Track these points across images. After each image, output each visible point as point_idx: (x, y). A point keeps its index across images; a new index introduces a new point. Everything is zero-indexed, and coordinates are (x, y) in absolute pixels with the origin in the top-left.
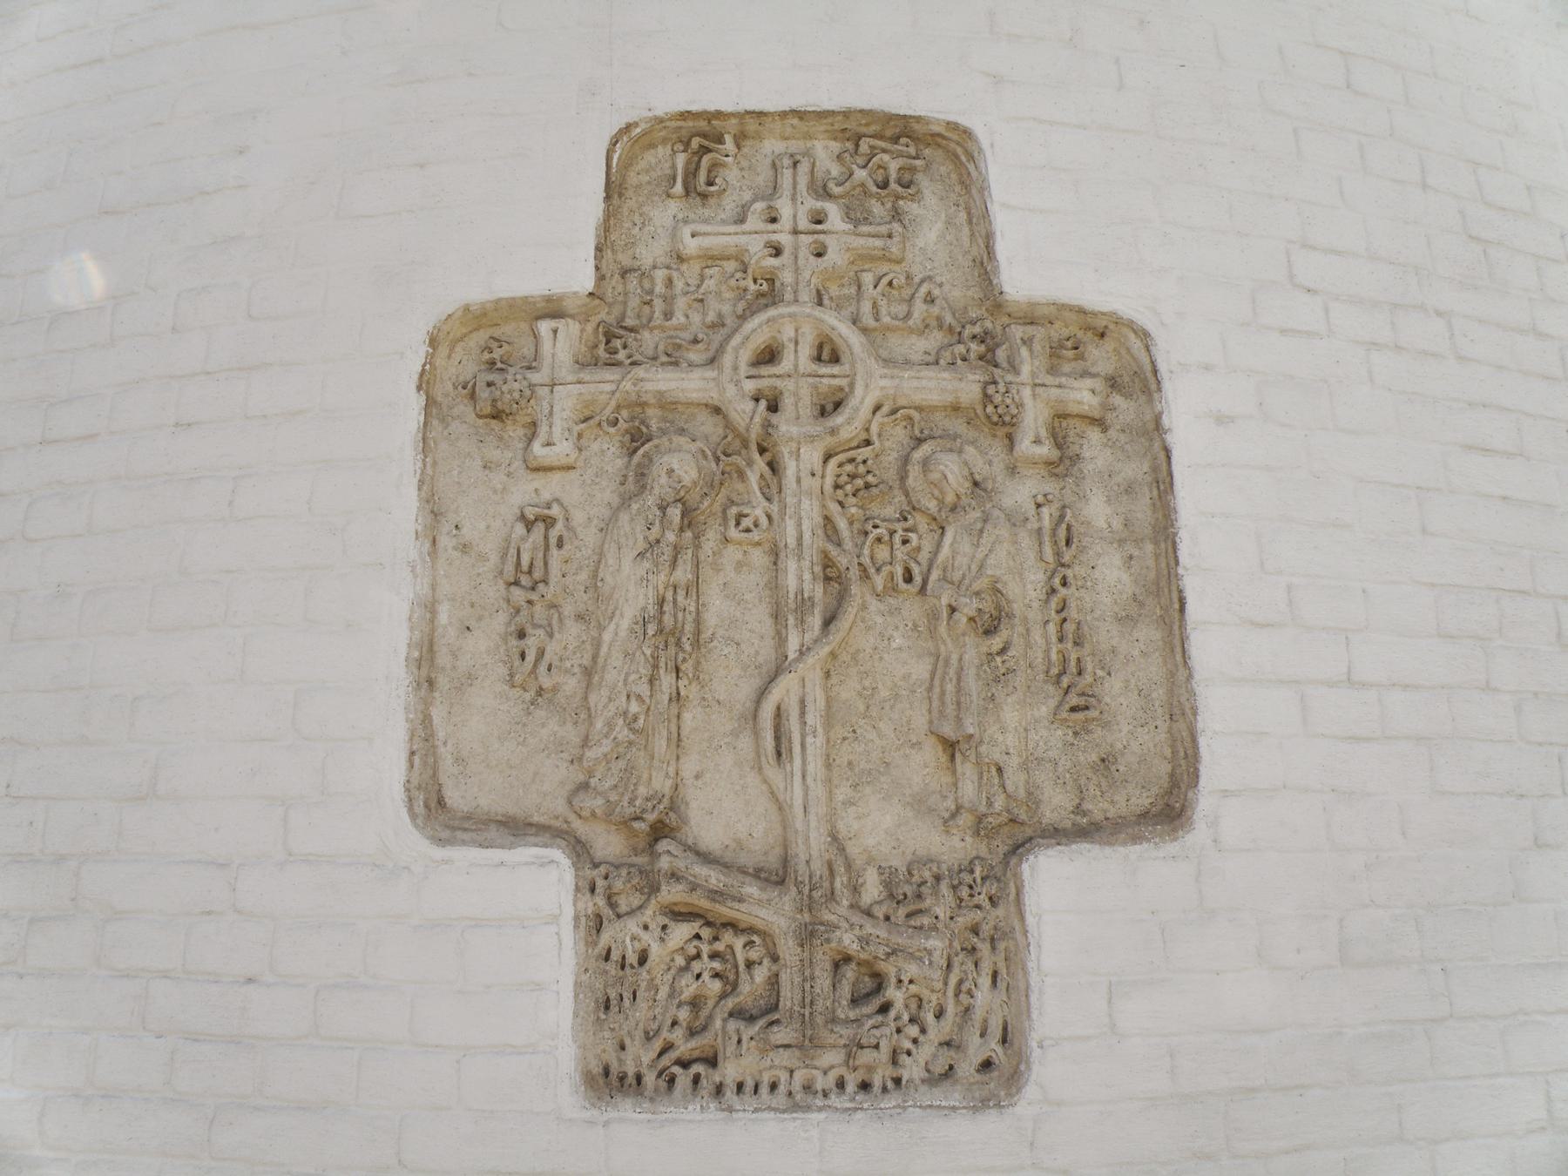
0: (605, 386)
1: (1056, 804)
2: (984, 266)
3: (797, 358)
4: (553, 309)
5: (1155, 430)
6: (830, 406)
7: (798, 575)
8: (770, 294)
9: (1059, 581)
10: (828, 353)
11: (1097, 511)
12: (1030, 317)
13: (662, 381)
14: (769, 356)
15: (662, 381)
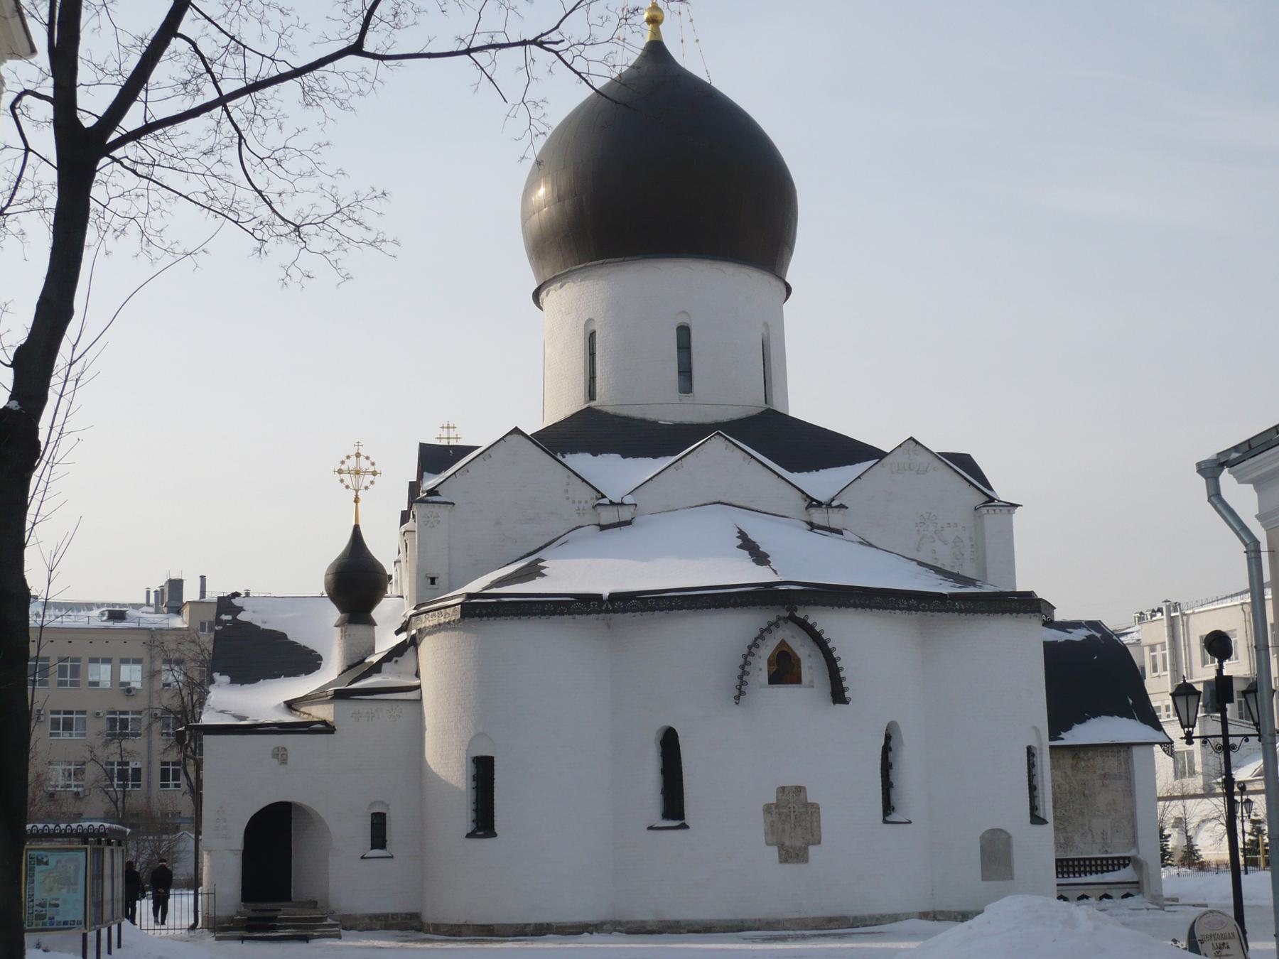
0: (777, 811)
1: (811, 843)
2: (806, 799)
3: (792, 808)
4: (773, 804)
5: (819, 813)
6: (794, 812)
7: (792, 826)
8: (789, 803)
9: (811, 826)
10: (794, 807)
11: (814, 819)
12: (810, 803)
13: (781, 810)
14: (790, 808)
15: (781, 810)
